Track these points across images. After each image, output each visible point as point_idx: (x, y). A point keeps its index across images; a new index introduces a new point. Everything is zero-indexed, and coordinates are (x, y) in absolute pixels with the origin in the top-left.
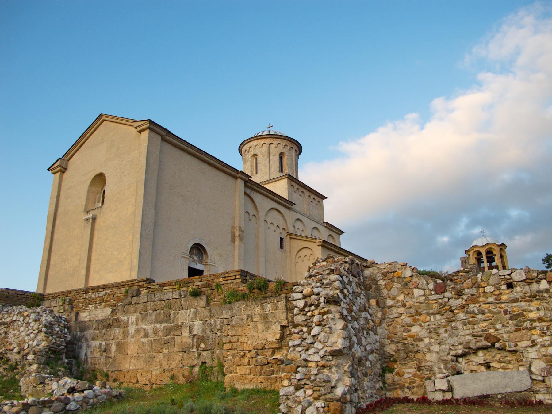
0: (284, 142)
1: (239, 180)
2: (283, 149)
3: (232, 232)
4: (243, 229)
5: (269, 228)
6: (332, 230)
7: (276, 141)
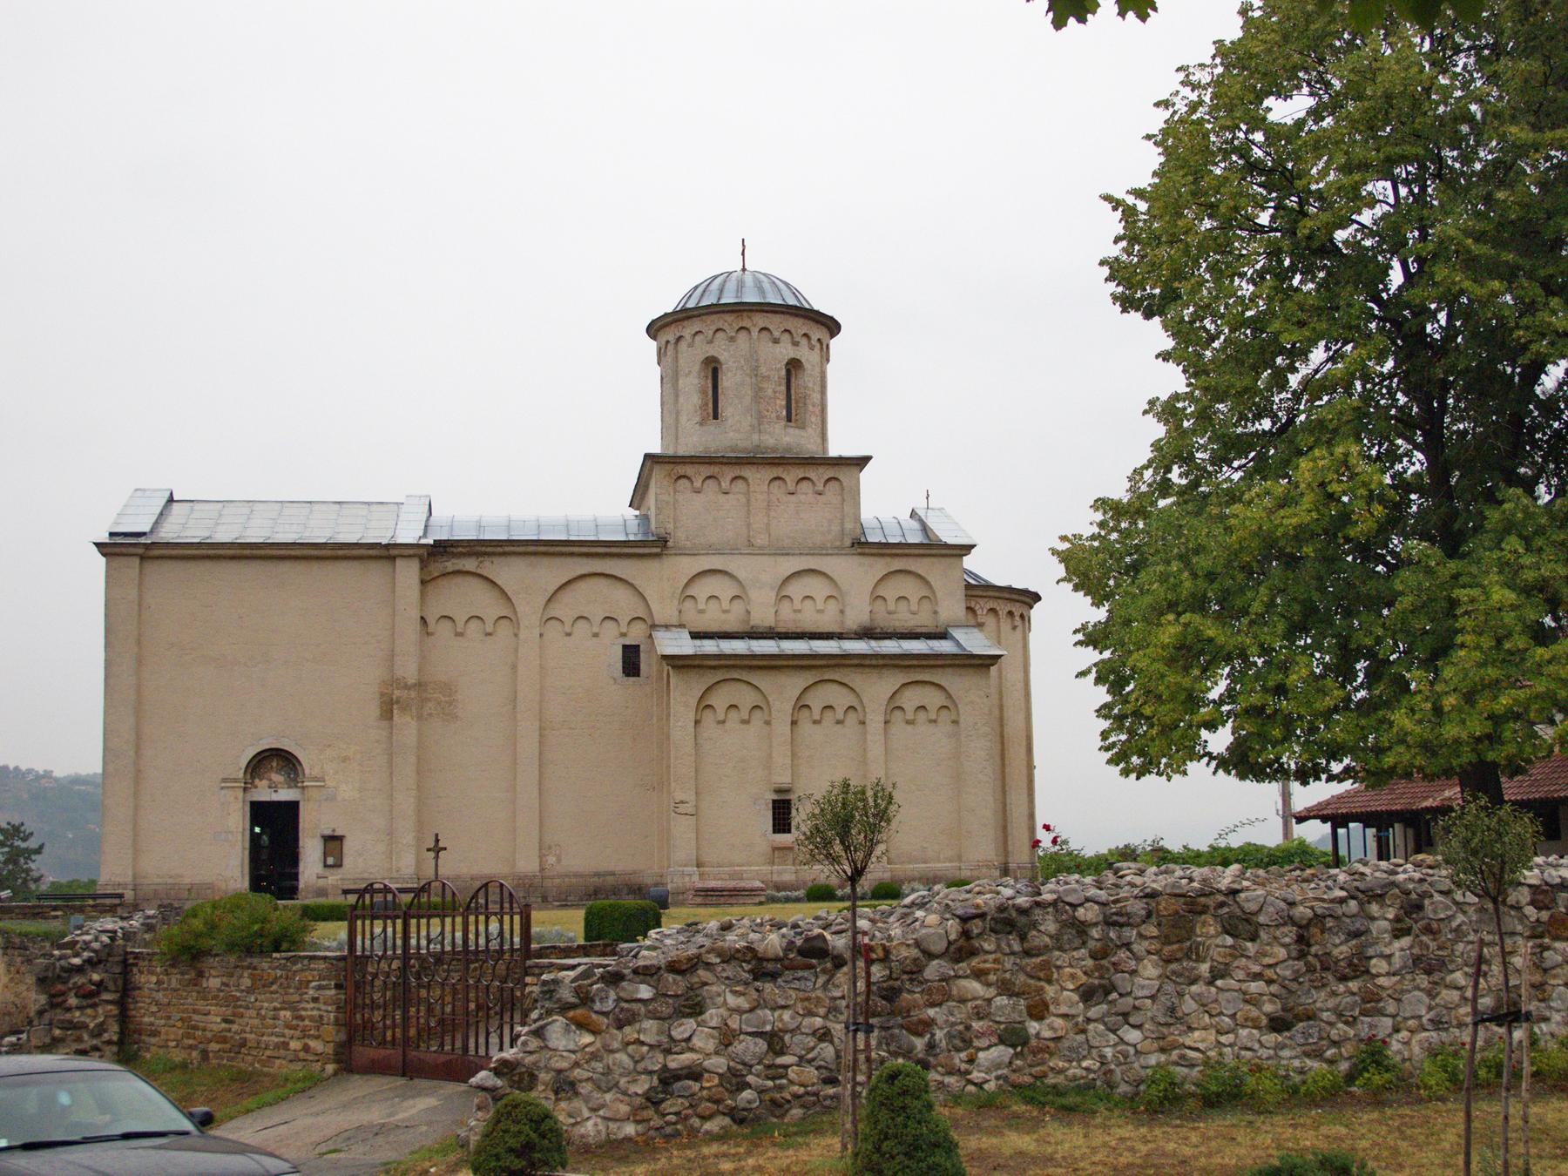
0: (708, 325)
1: (399, 562)
2: (708, 348)
3: (382, 695)
4: (411, 681)
5: (569, 635)
7: (688, 330)
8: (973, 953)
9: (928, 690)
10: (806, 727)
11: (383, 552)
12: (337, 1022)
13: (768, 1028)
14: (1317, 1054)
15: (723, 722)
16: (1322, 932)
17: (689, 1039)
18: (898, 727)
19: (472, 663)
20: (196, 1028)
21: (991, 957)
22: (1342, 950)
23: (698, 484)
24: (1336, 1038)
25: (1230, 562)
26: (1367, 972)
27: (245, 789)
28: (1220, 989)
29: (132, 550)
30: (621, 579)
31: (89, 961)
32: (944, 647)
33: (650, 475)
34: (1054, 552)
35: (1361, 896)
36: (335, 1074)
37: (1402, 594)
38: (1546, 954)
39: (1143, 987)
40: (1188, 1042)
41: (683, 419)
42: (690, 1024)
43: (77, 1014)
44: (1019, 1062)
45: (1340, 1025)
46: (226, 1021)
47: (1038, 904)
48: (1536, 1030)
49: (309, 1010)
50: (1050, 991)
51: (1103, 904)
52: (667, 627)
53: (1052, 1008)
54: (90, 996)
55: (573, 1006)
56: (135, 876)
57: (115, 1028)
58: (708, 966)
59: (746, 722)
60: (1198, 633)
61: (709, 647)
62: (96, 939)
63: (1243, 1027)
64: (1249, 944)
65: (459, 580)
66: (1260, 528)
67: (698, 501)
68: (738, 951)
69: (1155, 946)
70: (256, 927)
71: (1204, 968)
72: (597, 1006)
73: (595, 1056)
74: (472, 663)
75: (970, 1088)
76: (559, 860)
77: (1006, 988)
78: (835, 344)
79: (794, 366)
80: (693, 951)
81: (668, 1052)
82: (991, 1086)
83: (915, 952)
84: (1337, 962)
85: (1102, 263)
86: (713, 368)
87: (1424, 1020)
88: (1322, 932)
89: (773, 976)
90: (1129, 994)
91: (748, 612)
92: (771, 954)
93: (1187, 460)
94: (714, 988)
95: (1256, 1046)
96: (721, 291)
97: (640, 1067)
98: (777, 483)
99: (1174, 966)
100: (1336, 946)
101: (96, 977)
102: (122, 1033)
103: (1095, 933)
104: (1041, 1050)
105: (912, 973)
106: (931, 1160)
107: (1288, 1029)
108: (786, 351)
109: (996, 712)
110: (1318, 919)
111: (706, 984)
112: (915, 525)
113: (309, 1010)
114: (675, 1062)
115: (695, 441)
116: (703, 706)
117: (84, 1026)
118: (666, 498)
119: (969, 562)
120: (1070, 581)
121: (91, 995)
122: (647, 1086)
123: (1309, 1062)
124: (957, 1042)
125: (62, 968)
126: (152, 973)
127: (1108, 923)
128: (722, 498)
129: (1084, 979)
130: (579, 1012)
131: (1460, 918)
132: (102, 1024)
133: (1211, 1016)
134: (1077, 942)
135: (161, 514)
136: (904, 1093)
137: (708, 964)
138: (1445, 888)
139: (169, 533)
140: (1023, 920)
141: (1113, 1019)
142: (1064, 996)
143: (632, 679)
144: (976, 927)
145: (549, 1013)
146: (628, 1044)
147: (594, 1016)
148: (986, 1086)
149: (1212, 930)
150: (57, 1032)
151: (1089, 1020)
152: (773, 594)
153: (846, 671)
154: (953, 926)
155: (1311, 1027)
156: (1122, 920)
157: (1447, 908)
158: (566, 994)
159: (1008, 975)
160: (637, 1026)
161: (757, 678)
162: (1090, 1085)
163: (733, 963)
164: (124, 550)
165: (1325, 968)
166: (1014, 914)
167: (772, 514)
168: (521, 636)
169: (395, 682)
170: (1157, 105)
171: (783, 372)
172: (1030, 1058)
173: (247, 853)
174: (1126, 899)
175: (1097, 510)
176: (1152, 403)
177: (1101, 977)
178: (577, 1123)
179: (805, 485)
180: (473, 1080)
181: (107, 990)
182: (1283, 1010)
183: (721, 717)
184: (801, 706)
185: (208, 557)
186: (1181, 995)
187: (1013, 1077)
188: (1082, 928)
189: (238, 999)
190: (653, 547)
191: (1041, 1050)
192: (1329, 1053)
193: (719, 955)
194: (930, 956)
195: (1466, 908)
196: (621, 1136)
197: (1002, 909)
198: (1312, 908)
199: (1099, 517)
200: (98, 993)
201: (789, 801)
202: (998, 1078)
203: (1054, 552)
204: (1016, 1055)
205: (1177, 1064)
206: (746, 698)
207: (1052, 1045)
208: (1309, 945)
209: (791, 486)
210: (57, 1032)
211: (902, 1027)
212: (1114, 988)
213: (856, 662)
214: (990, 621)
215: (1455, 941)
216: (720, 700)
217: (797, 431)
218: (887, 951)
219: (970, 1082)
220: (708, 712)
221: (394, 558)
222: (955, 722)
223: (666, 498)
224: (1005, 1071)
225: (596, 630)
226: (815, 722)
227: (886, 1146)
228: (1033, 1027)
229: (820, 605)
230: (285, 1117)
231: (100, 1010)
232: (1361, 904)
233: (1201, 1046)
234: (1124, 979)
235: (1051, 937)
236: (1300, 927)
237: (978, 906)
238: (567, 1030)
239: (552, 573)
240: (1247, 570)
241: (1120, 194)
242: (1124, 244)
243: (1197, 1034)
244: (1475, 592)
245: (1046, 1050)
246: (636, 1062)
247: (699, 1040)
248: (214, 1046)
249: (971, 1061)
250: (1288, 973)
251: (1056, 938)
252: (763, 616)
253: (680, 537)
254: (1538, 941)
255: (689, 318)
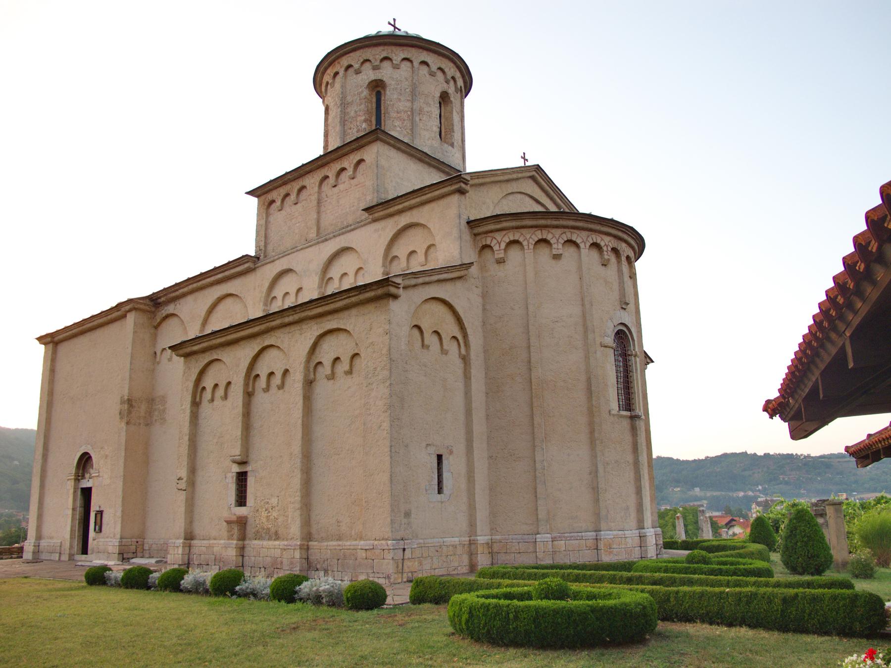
1: (128, 315)
6: (411, 208)
108: (369, 75)
153: (279, 333)
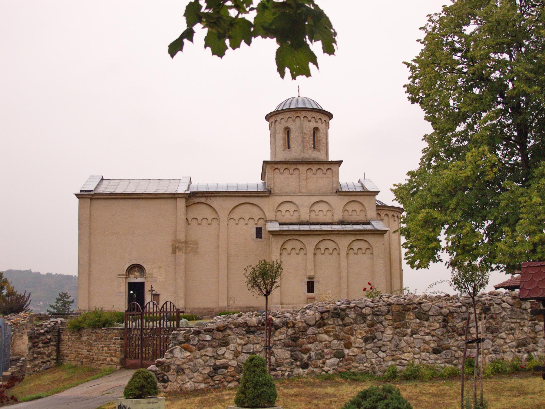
0: (286, 116)
3: (173, 245)
4: (182, 241)
5: (237, 224)
7: (279, 118)
8: (324, 325)
9: (362, 242)
10: (319, 256)
11: (173, 196)
12: (121, 351)
13: (252, 351)
14: (450, 362)
15: (290, 254)
16: (453, 318)
17: (224, 354)
18: (352, 256)
19: (204, 234)
20: (79, 354)
21: (331, 326)
22: (460, 324)
23: (282, 171)
24: (457, 356)
25: (443, 190)
26: (469, 332)
27: (126, 278)
28: (414, 338)
29: (87, 196)
30: (253, 204)
31: (46, 331)
32: (368, 227)
33: (266, 168)
34: (392, 190)
35: (467, 305)
36: (120, 369)
37: (502, 200)
38: (536, 326)
39: (386, 337)
40: (403, 357)
41: (278, 149)
42: (224, 349)
43: (42, 349)
44: (341, 364)
45: (459, 352)
46: (88, 351)
47: (348, 307)
48: (532, 354)
49: (113, 347)
50: (353, 338)
51: (372, 308)
52: (271, 221)
53: (353, 345)
54: (46, 343)
55: (184, 343)
56: (89, 307)
57: (55, 354)
58: (230, 328)
59: (298, 254)
60: (432, 216)
61: (285, 228)
62: (49, 324)
63: (423, 352)
64: (425, 322)
65: (199, 205)
66: (453, 177)
67: (282, 177)
68: (241, 323)
69: (391, 322)
70: (96, 319)
71: (409, 331)
72: (192, 343)
73: (191, 360)
74: (204, 234)
75: (323, 373)
76: (234, 302)
77: (337, 337)
78: (331, 122)
79: (316, 129)
80: (226, 323)
81: (216, 359)
82: (331, 372)
83: (304, 324)
84: (458, 329)
85: (404, 86)
86: (287, 131)
87: (490, 350)
88: (453, 318)
89: (253, 332)
90: (381, 340)
91: (300, 216)
92: (252, 325)
93: (438, 156)
94: (233, 337)
95: (428, 359)
96: (290, 104)
97: (206, 364)
98: (309, 170)
99: (398, 330)
100: (458, 323)
101: (49, 337)
102: (57, 356)
103: (369, 318)
104: (349, 360)
105: (302, 332)
106: (262, 390)
107: (440, 353)
108: (313, 124)
109: (388, 250)
110: (451, 313)
111: (230, 335)
112: (360, 185)
113: (113, 347)
114: (218, 362)
115: (282, 156)
116: (283, 248)
117: (44, 353)
118: (271, 176)
119: (377, 197)
120: (397, 200)
121: (46, 343)
122: (209, 371)
123: (447, 365)
124: (319, 357)
125: (37, 334)
126: (67, 335)
127: (374, 314)
128: (290, 176)
129: (365, 334)
130: (185, 344)
131: (504, 313)
132: (51, 352)
133: (411, 348)
134: (362, 321)
135: (99, 184)
136: (255, 366)
137: (230, 328)
138: (499, 302)
139: (101, 190)
140: (343, 313)
141: (376, 348)
142: (357, 340)
143: (259, 239)
144: (326, 315)
145: (175, 345)
146: (202, 356)
147: (190, 346)
148: (329, 372)
149: (412, 318)
150: (35, 355)
151: (367, 349)
152: (308, 210)
153: (333, 236)
154: (318, 316)
155: (448, 352)
156: (378, 313)
157: (499, 309)
158: (181, 338)
159: (337, 333)
160: (206, 350)
161: (301, 239)
162: (367, 373)
163: (239, 328)
164: (85, 196)
165: (454, 331)
166: (340, 311)
167: (308, 181)
168: (221, 225)
169: (177, 241)
170: (420, 29)
171: (312, 132)
172: (345, 363)
173: (127, 300)
174: (381, 306)
175: (409, 175)
176: (425, 136)
177: (371, 334)
178: (184, 383)
179: (319, 171)
180: (149, 368)
181: (52, 341)
182: (438, 346)
183: (289, 252)
184: (317, 248)
185: (113, 198)
186: (400, 340)
187: (339, 369)
188: (364, 317)
189: (92, 344)
190: (267, 193)
191: (349, 360)
192: (454, 362)
193: (234, 325)
194: (309, 326)
195: (506, 310)
196: (199, 388)
197: (335, 309)
198: (449, 309)
199: (409, 177)
200: (49, 342)
201: (313, 282)
202: (333, 369)
203: (392, 190)
204: (340, 361)
205: (398, 365)
206: (298, 245)
207: (353, 358)
208: (448, 323)
209: (315, 172)
210: (35, 355)
211: (299, 351)
212: (376, 338)
213: (336, 232)
214: (386, 218)
215: (502, 322)
216: (289, 246)
217: (317, 152)
218: (294, 324)
219: (323, 371)
220: (284, 251)
221: (176, 198)
222: (372, 254)
223: (271, 176)
224: (336, 367)
225: (247, 222)
226: (322, 254)
227: (247, 385)
228: (346, 351)
229: (325, 213)
230: (98, 383)
231: (50, 348)
232: (467, 308)
233: (407, 359)
234: (379, 335)
235: (353, 319)
236: (445, 316)
237: (327, 308)
238: (181, 351)
239: (231, 203)
240: (450, 193)
241: (410, 62)
242: (411, 79)
243: (406, 354)
244: (527, 198)
245: (351, 359)
246: (205, 362)
247: (227, 355)
248: (85, 360)
249: (324, 363)
250: (440, 333)
251: (355, 319)
252: (305, 217)
253: (276, 190)
254: (533, 322)
255: (279, 113)
